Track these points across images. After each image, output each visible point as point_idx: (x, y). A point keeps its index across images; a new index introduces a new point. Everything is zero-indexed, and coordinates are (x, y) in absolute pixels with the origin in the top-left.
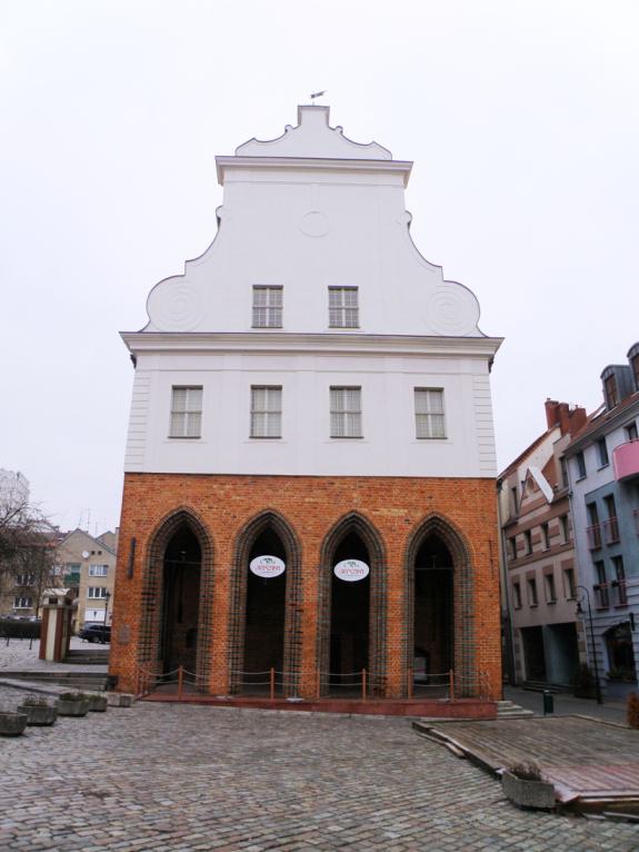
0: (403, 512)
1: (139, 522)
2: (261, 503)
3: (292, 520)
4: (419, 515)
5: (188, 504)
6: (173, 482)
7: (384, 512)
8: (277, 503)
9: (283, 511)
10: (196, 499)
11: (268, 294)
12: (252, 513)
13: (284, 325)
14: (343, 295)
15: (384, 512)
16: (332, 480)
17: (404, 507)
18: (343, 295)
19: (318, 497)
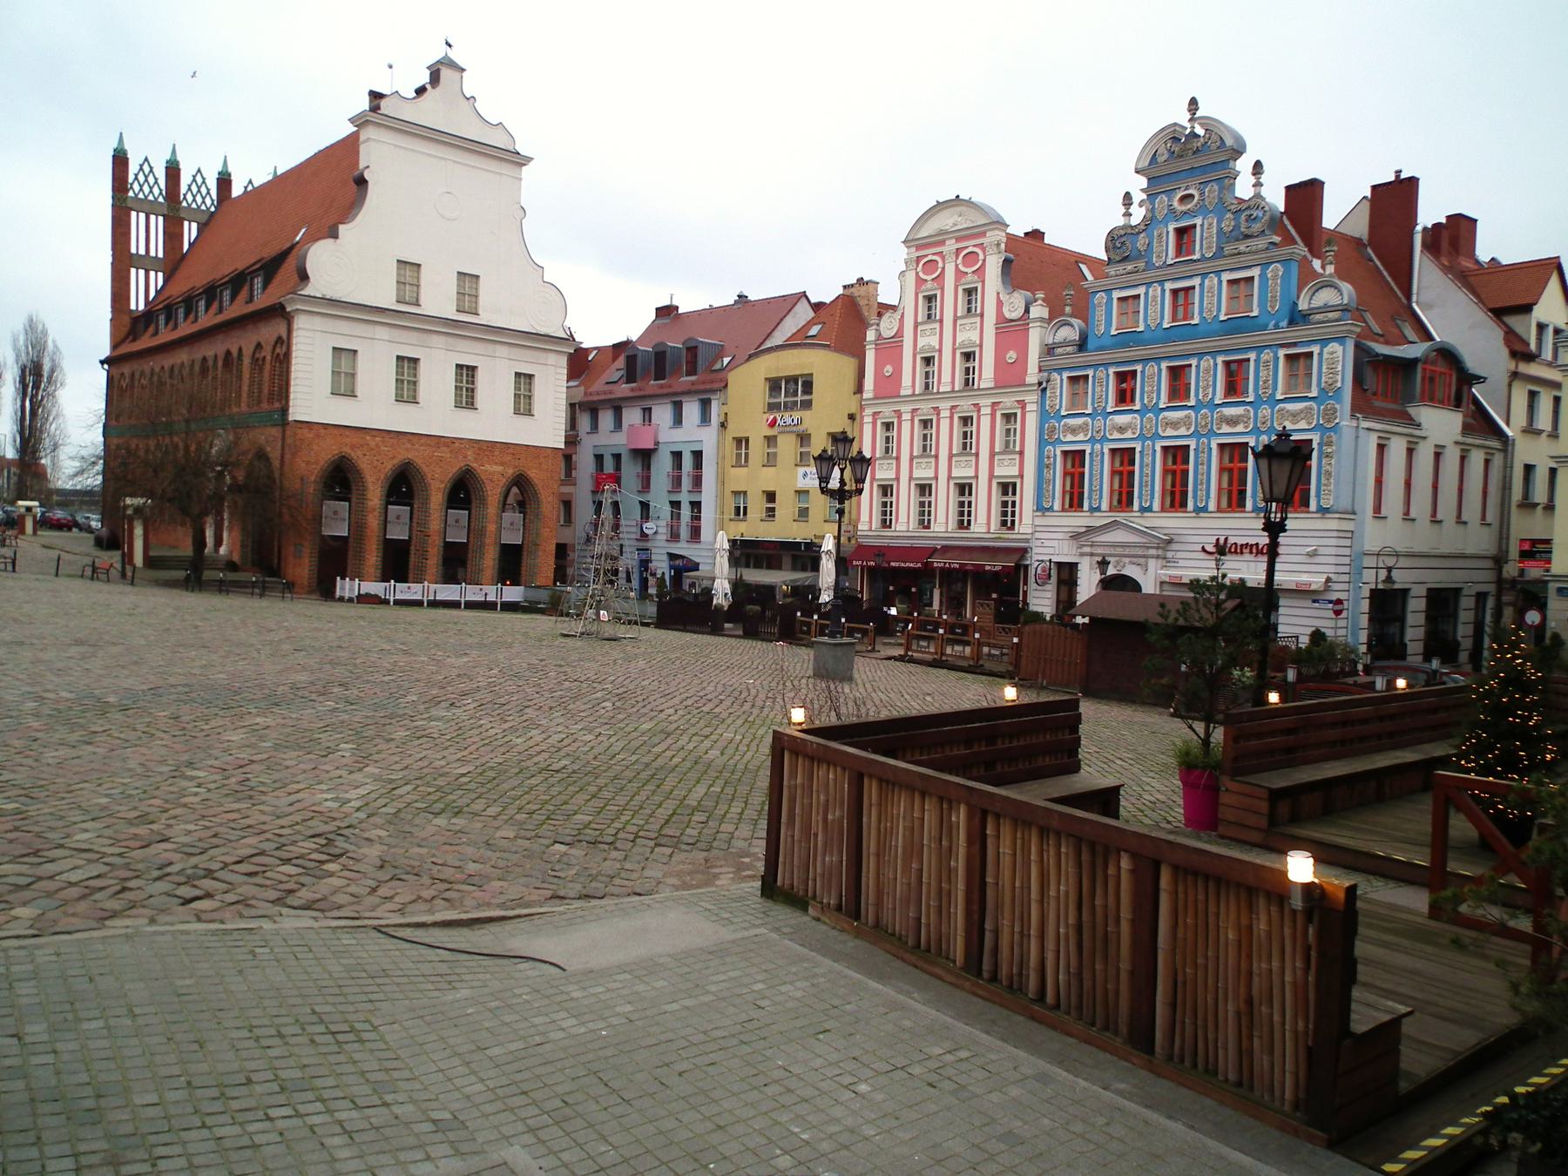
0: (500, 468)
1: (308, 463)
2: (403, 454)
3: (425, 469)
4: (511, 471)
5: (347, 450)
6: (336, 431)
7: (488, 467)
8: (417, 455)
9: (419, 462)
10: (353, 447)
11: (409, 270)
12: (395, 461)
13: (422, 301)
14: (468, 281)
15: (488, 467)
16: (453, 440)
17: (502, 464)
18: (468, 281)
19: (444, 453)
